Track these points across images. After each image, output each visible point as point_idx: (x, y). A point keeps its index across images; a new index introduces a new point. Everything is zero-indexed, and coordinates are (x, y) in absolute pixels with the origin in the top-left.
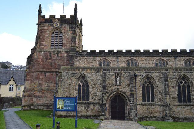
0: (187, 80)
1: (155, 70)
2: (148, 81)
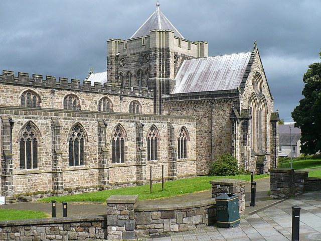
0: (80, 131)
1: (41, 114)
2: (29, 133)
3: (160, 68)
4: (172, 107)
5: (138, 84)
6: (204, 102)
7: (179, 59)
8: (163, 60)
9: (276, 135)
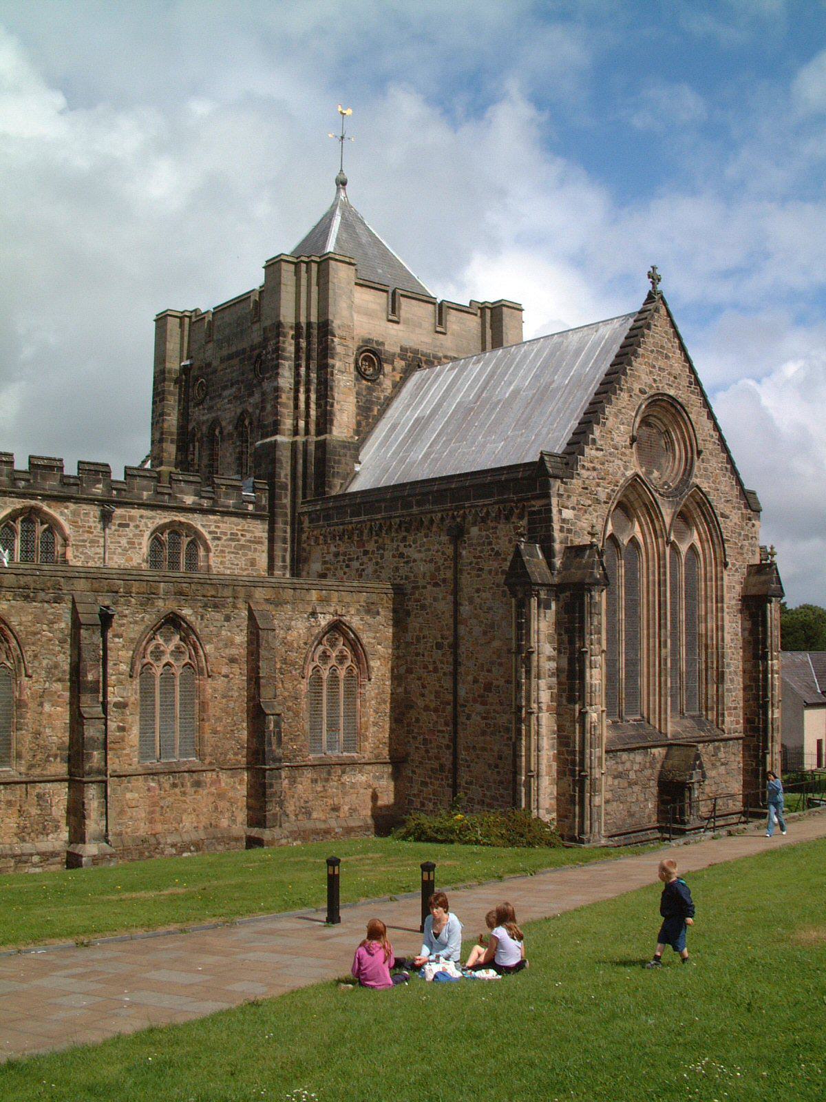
3: (296, 399)
4: (333, 549)
5: (241, 465)
6: (432, 521)
7: (387, 368)
8: (308, 368)
9: (764, 657)
